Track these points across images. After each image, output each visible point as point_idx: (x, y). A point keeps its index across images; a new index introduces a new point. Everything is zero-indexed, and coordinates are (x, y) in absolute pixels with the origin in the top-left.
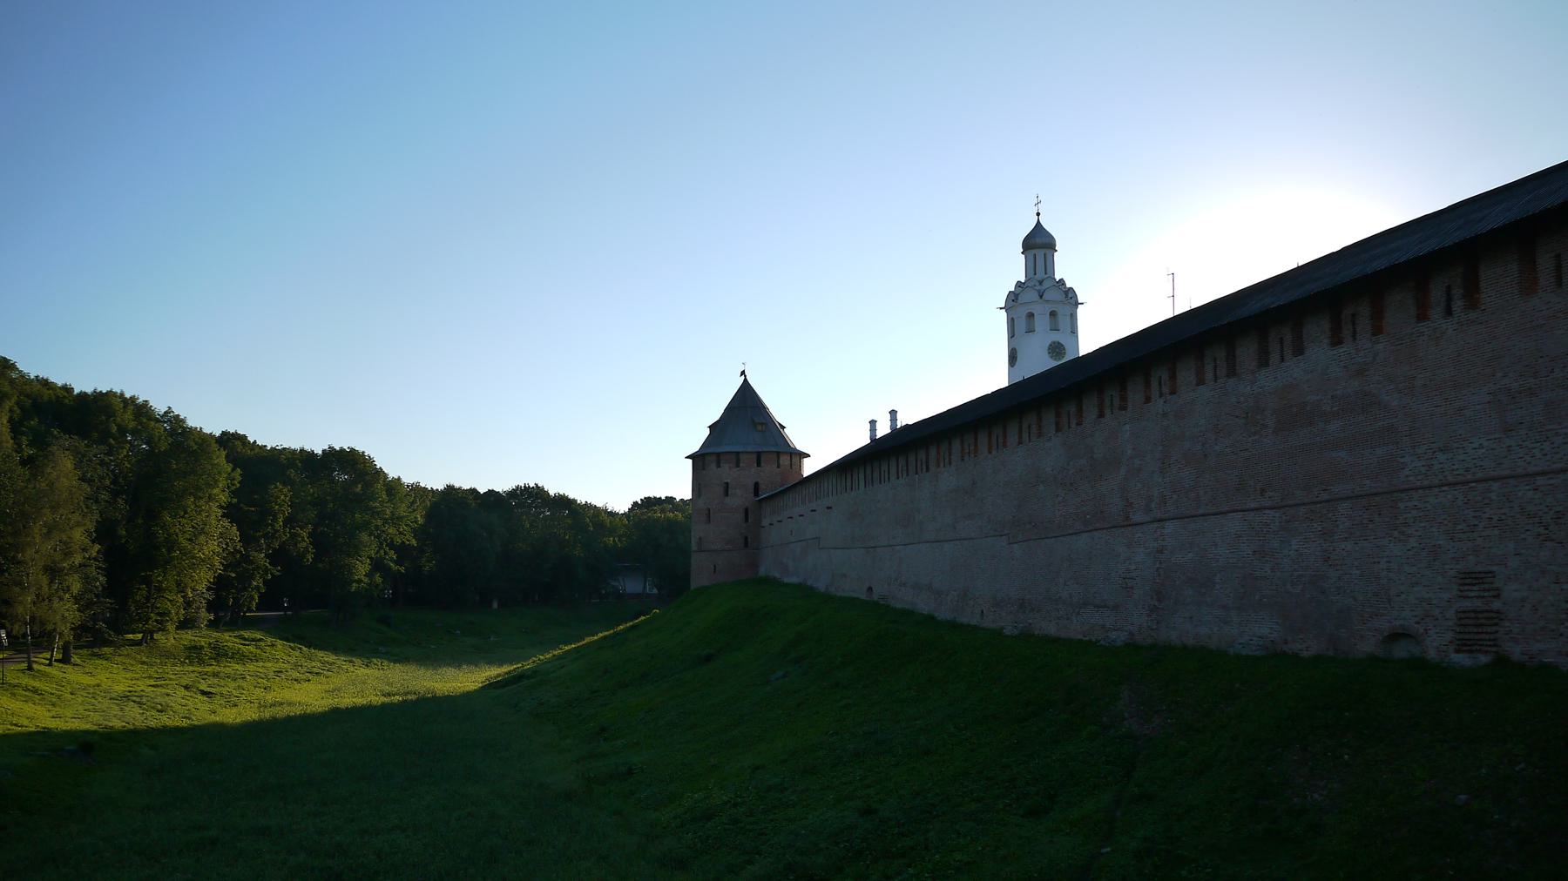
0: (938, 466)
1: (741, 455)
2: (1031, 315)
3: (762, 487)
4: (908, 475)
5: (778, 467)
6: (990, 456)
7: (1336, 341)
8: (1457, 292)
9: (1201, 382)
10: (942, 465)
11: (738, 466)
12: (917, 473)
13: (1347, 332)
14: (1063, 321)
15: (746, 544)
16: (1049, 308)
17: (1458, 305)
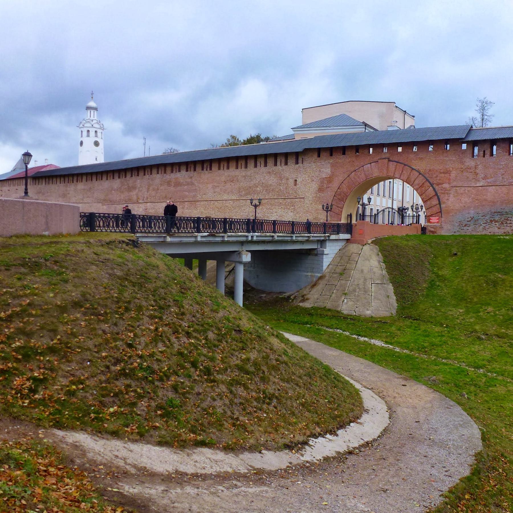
0: (77, 182)
2: (88, 131)
7: (187, 171)
8: (209, 167)
9: (158, 173)
13: (189, 170)
14: (99, 134)
16: (95, 129)
17: (208, 169)
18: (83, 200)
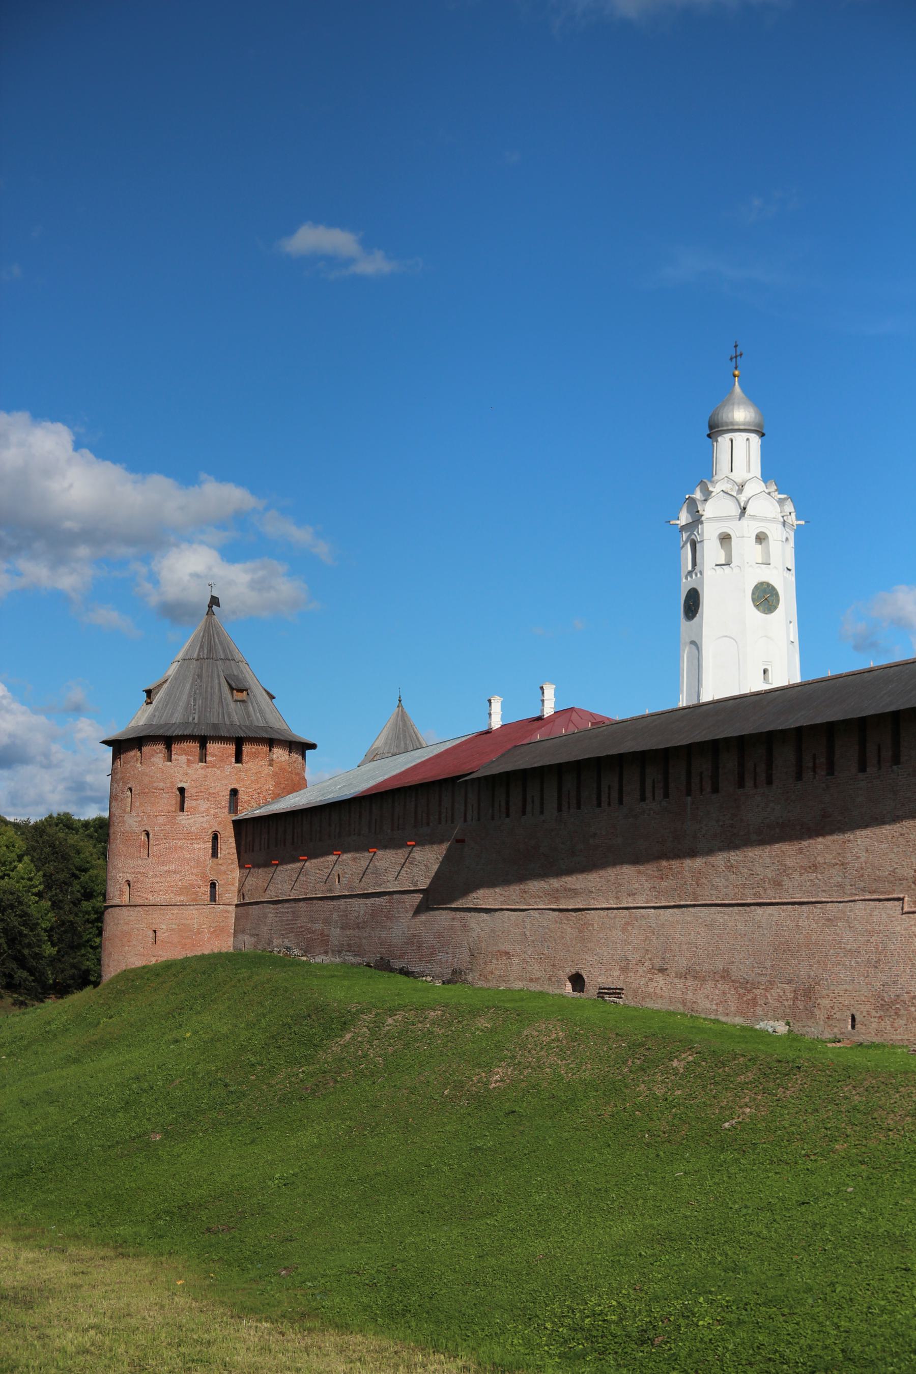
0: (741, 784)
1: (211, 746)
2: (725, 539)
3: (242, 796)
4: (666, 795)
5: (271, 763)
6: (861, 776)
10: (749, 783)
11: (203, 758)
12: (689, 793)
15: (213, 898)
18: (778, 884)
